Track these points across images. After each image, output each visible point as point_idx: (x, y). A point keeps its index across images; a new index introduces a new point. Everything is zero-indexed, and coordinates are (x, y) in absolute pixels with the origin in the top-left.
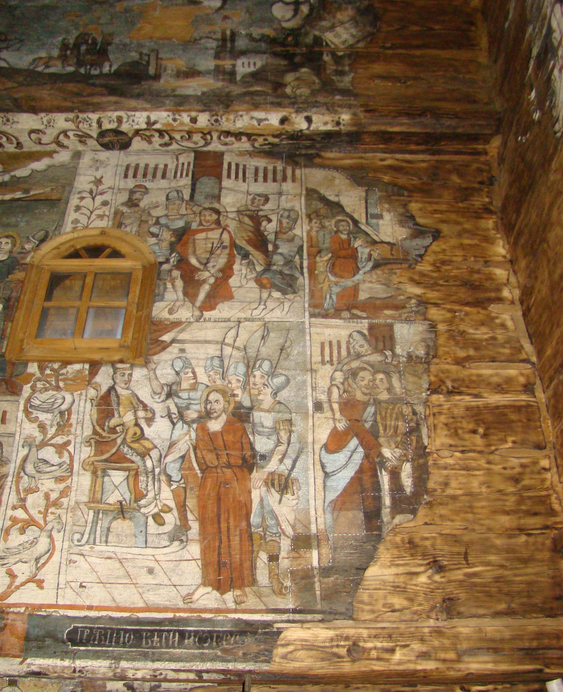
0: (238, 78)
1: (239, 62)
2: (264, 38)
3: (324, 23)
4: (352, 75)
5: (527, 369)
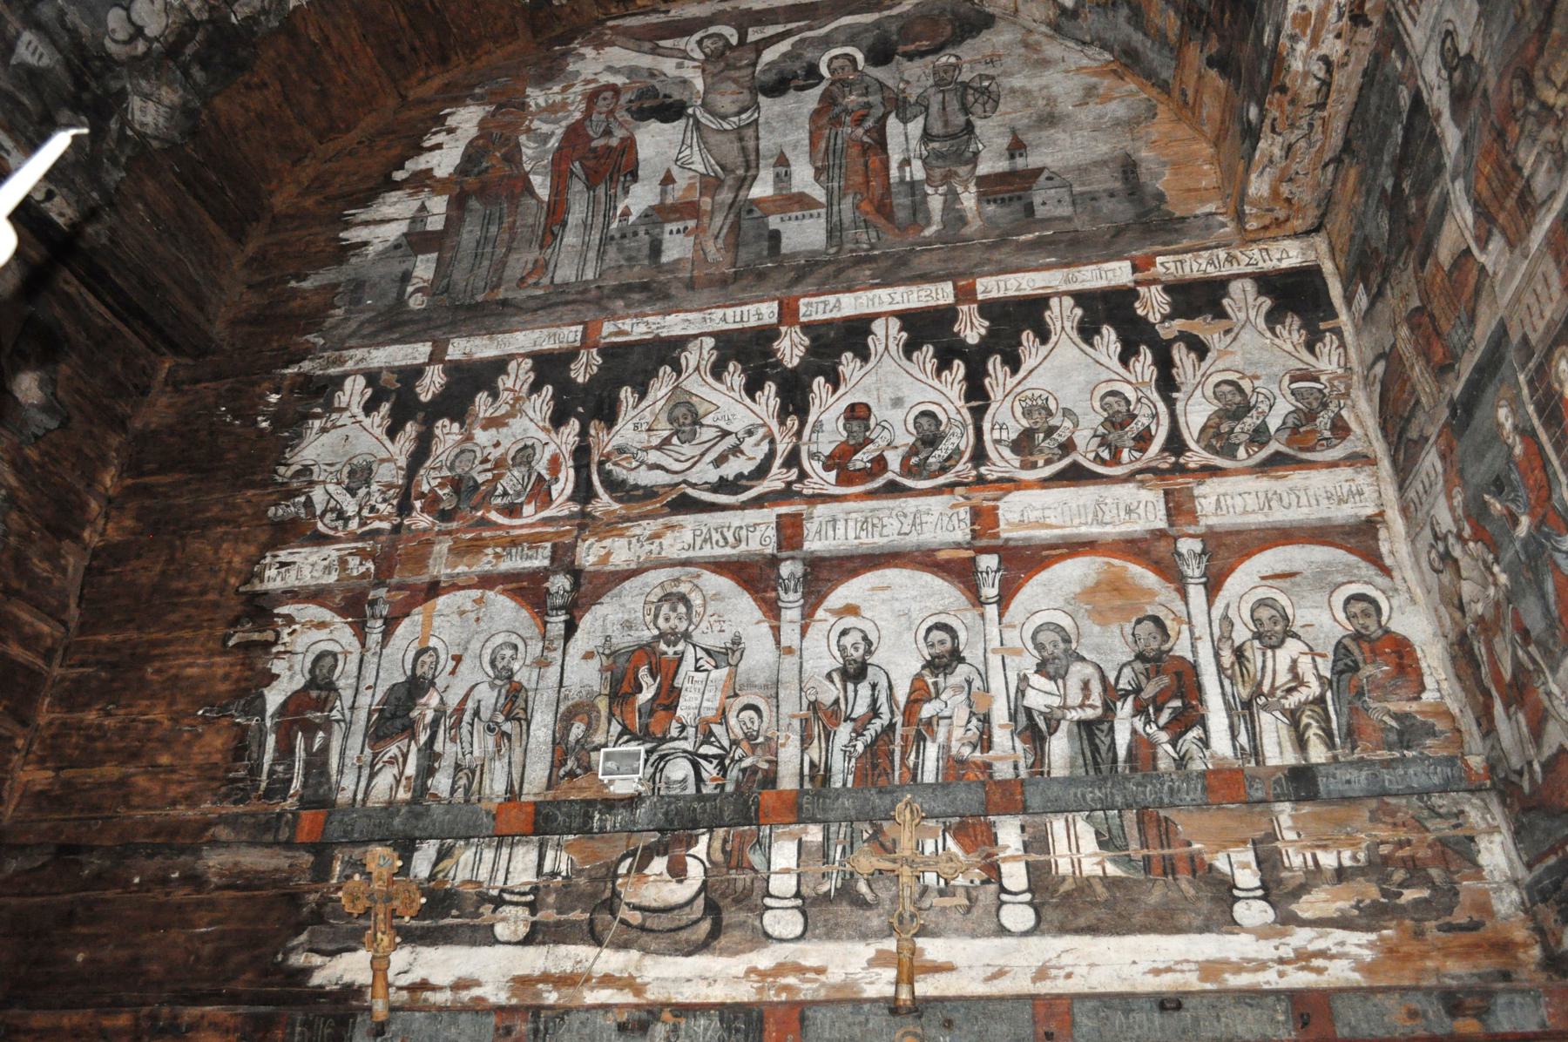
0: (13, 61)
1: (27, 36)
2: (73, 32)
3: (143, 83)
4: (123, 174)
5: (59, 632)
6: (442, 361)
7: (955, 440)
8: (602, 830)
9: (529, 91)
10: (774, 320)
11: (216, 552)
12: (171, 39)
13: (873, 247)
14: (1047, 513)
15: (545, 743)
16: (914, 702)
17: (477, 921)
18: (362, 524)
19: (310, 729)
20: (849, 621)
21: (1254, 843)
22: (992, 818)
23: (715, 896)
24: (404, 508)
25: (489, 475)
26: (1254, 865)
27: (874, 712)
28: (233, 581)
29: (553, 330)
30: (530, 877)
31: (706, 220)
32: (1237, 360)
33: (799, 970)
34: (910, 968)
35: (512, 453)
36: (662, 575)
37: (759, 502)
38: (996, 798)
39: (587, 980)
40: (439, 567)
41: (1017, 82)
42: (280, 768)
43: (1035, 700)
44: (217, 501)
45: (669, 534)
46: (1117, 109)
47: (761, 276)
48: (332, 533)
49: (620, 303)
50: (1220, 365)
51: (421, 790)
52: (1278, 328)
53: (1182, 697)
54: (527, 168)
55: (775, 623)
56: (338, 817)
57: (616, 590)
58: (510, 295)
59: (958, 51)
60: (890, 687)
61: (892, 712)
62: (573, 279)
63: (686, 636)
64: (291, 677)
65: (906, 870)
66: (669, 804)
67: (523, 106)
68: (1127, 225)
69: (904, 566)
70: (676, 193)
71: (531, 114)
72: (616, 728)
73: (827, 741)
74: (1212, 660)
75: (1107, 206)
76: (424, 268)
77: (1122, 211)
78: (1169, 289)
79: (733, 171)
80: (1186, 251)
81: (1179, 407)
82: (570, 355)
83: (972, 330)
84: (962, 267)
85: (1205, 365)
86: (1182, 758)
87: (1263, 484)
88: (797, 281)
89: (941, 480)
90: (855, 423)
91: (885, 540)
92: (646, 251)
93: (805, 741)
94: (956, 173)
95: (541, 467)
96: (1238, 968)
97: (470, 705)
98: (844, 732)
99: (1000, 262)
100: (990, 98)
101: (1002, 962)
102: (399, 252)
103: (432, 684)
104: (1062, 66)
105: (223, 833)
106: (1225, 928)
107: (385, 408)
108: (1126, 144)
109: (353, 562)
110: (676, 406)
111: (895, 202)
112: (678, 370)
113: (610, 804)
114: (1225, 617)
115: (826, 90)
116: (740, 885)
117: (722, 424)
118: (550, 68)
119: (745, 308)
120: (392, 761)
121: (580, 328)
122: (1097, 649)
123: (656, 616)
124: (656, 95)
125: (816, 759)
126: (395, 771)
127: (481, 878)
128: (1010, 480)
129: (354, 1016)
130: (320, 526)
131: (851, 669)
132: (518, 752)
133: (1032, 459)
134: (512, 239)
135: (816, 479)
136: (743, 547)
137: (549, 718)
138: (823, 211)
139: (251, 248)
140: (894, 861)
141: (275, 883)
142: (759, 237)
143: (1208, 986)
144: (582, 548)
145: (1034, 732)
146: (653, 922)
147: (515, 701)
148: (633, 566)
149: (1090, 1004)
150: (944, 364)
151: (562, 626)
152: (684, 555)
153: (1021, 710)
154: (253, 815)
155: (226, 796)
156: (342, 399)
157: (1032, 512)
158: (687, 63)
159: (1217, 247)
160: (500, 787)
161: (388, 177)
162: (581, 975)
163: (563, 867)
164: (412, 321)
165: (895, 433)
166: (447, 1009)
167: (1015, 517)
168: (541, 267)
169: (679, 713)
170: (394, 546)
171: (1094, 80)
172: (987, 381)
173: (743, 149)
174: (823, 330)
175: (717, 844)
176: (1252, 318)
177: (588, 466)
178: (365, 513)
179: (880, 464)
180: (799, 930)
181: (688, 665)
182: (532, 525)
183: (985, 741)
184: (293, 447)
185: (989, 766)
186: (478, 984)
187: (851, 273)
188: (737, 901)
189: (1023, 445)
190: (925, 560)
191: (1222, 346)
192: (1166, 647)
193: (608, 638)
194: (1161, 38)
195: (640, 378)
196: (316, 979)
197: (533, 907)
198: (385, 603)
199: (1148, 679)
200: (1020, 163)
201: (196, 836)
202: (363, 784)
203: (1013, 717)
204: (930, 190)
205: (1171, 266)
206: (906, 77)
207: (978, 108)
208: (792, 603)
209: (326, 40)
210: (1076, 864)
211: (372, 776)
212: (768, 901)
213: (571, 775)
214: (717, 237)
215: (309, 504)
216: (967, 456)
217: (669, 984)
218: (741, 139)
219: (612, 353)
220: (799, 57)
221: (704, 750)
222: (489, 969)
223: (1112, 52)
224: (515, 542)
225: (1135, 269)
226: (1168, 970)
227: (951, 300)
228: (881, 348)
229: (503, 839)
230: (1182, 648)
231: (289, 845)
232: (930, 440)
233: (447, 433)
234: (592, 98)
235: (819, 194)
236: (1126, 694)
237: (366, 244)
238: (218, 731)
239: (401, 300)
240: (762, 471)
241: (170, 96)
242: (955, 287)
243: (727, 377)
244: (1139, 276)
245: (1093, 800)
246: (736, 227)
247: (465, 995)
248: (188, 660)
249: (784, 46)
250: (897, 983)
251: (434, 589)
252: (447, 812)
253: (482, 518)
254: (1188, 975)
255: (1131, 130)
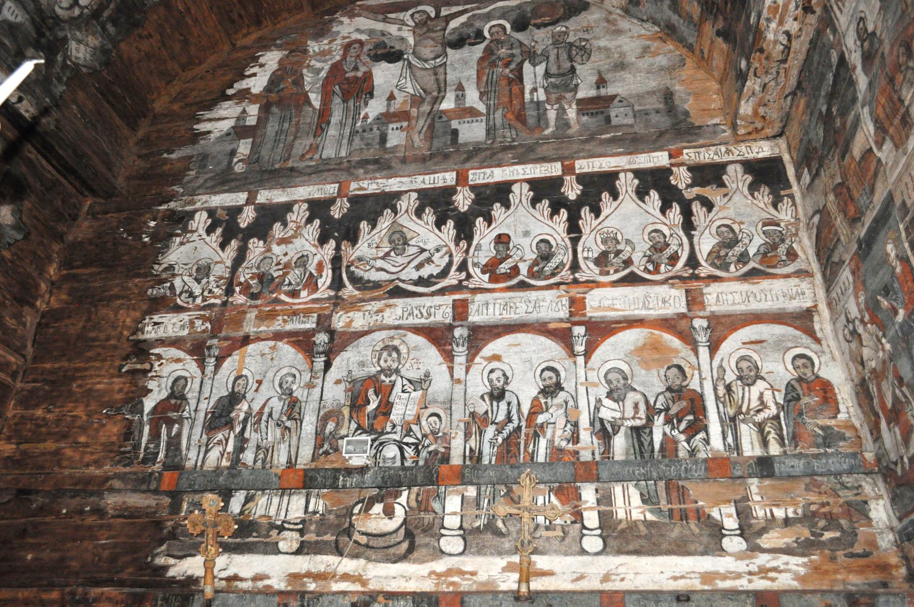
3: (78, 33)
4: (65, 88)
5: (21, 362)
6: (253, 204)
7: (560, 257)
8: (344, 487)
9: (309, 42)
10: (454, 183)
11: (116, 315)
12: (95, 7)
13: (514, 140)
14: (615, 302)
15: (311, 434)
16: (533, 414)
17: (268, 540)
18: (204, 300)
19: (170, 423)
20: (495, 364)
21: (735, 502)
22: (578, 484)
23: (411, 527)
24: (229, 291)
25: (281, 273)
26: (735, 515)
27: (509, 419)
28: (125, 333)
29: (321, 186)
30: (300, 514)
31: (414, 122)
32: (731, 213)
33: (461, 573)
34: (527, 573)
35: (294, 260)
36: (384, 334)
37: (442, 292)
38: (581, 472)
39: (334, 576)
40: (250, 327)
41: (602, 43)
42: (152, 446)
43: (605, 414)
44: (117, 285)
45: (388, 310)
46: (662, 60)
47: (446, 156)
48: (185, 305)
49: (361, 171)
50: (721, 215)
51: (236, 461)
52: (756, 193)
53: (694, 413)
54: (307, 89)
55: (450, 365)
56: (186, 476)
57: (355, 343)
58: (295, 165)
59: (567, 24)
60: (519, 404)
61: (520, 419)
62: (333, 156)
63: (397, 371)
64: (160, 391)
65: (526, 514)
66: (385, 472)
67: (305, 51)
68: (666, 130)
69: (529, 332)
70: (396, 106)
71: (310, 56)
72: (354, 426)
73: (480, 436)
74: (712, 392)
75: (654, 118)
76: (244, 148)
77: (664, 122)
78: (691, 169)
79: (430, 93)
80: (701, 146)
81: (696, 240)
82: (331, 201)
83: (572, 191)
84: (567, 153)
85: (711, 215)
86: (693, 451)
87: (745, 287)
88: (467, 160)
89: (552, 281)
90: (501, 245)
91: (517, 316)
92: (377, 140)
93: (467, 436)
94: (564, 97)
95: (312, 268)
96: (724, 577)
97: (267, 410)
98: (490, 431)
99: (589, 151)
100: (586, 52)
101: (582, 571)
102: (229, 138)
103: (244, 397)
104: (630, 34)
105: (117, 484)
106: (717, 553)
107: (219, 231)
108: (666, 81)
109: (198, 323)
110: (393, 233)
111: (528, 113)
112: (395, 212)
113: (349, 471)
114: (721, 367)
115: (487, 46)
116: (426, 522)
117: (421, 245)
118: (322, 29)
119: (436, 176)
120: (219, 443)
121: (337, 185)
122: (643, 384)
123: (379, 359)
124: (385, 47)
125: (473, 447)
126: (221, 449)
127: (271, 514)
128: (593, 282)
129: (193, 595)
130: (179, 301)
131: (495, 393)
132: (294, 442)
133: (607, 269)
134: (297, 131)
135: (477, 279)
136: (432, 319)
137: (314, 419)
138: (484, 118)
139: (140, 134)
140: (519, 509)
141: (147, 515)
142: (445, 133)
143: (706, 587)
144: (335, 317)
145: (605, 433)
146: (373, 542)
147: (293, 408)
148: (366, 329)
149: (634, 597)
150: (555, 211)
151: (323, 364)
152: (397, 323)
153: (597, 419)
154: (135, 473)
155: (119, 462)
156: (193, 225)
157: (605, 301)
158: (404, 27)
159: (720, 144)
160: (283, 459)
161: (224, 92)
162: (329, 573)
163: (320, 508)
164: (236, 179)
165: (524, 252)
166: (249, 592)
167: (595, 304)
168: (314, 148)
169: (392, 417)
170: (223, 314)
171: (648, 43)
172: (580, 222)
173: (437, 80)
174: (483, 189)
175: (413, 497)
176: (740, 187)
177: (340, 268)
178: (206, 293)
179: (515, 270)
180: (461, 549)
181: (398, 389)
182: (306, 303)
183: (575, 438)
184: (163, 254)
185: (577, 453)
186: (268, 577)
187: (500, 156)
188: (424, 531)
189: (602, 260)
190: (541, 328)
191: (722, 204)
192: (684, 384)
193: (350, 372)
194: (689, 19)
195: (372, 216)
196: (171, 573)
197: (302, 532)
198: (217, 348)
199: (674, 402)
200: (603, 92)
201: (101, 485)
202: (201, 456)
203: (592, 424)
204: (548, 107)
205: (693, 155)
206: (535, 39)
207: (578, 58)
208: (461, 354)
209: (188, 10)
210: (628, 513)
211: (207, 452)
212: (443, 531)
213: (326, 453)
214: (420, 133)
215: (172, 287)
216: (567, 267)
217: (382, 580)
218: (436, 74)
219: (356, 201)
220: (472, 25)
221: (406, 440)
222: (275, 568)
223: (659, 26)
224: (295, 313)
225: (671, 156)
226: (682, 577)
227: (560, 173)
228: (517, 201)
229: (284, 491)
230: (694, 385)
231: (156, 492)
232: (545, 256)
233: (256, 247)
234: (347, 47)
235: (482, 108)
236: (661, 411)
237: (209, 132)
238: (115, 423)
239: (230, 166)
240: (444, 273)
241: (94, 41)
242: (562, 165)
243: (424, 216)
244: (673, 161)
245: (639, 474)
246: (431, 127)
247: (260, 584)
248: (98, 380)
249: (463, 19)
250: (520, 582)
251: (246, 340)
252: (252, 474)
253: (276, 298)
254: (694, 580)
255: (670, 73)
